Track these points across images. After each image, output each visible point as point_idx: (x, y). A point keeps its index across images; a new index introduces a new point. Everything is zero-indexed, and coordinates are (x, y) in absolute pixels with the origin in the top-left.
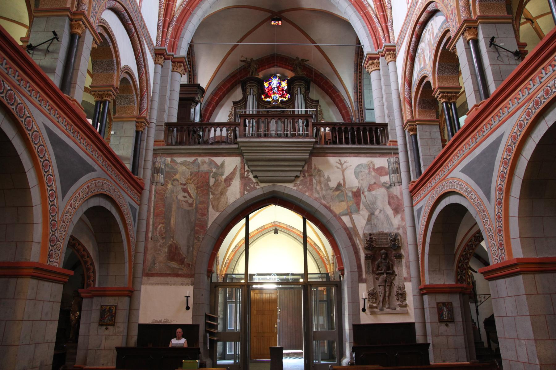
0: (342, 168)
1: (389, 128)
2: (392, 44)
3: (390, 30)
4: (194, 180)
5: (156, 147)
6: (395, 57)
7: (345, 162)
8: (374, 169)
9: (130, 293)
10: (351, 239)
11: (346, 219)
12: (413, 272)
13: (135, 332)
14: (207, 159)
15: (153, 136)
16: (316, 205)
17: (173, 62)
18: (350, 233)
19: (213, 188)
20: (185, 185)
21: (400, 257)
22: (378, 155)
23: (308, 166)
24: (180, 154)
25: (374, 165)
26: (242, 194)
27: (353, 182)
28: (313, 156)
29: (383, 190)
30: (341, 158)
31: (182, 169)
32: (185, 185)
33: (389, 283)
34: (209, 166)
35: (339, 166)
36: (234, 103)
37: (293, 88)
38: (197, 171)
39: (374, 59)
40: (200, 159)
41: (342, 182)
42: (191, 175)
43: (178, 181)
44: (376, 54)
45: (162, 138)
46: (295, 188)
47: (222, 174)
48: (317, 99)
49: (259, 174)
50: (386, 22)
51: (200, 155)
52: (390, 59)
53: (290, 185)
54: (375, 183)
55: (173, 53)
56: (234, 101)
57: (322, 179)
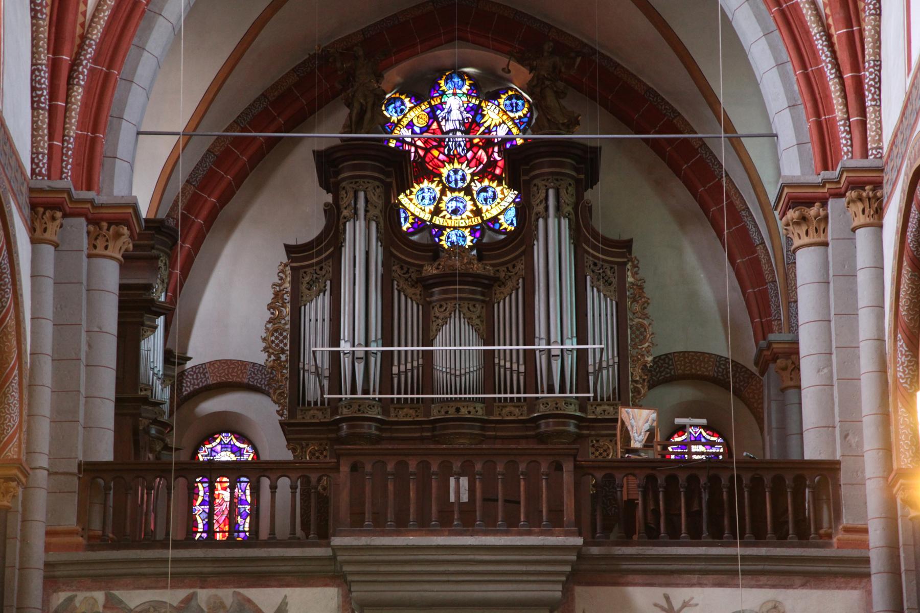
2: (871, 161)
17: (90, 221)
28: (580, 583)
39: (809, 202)
44: (817, 186)
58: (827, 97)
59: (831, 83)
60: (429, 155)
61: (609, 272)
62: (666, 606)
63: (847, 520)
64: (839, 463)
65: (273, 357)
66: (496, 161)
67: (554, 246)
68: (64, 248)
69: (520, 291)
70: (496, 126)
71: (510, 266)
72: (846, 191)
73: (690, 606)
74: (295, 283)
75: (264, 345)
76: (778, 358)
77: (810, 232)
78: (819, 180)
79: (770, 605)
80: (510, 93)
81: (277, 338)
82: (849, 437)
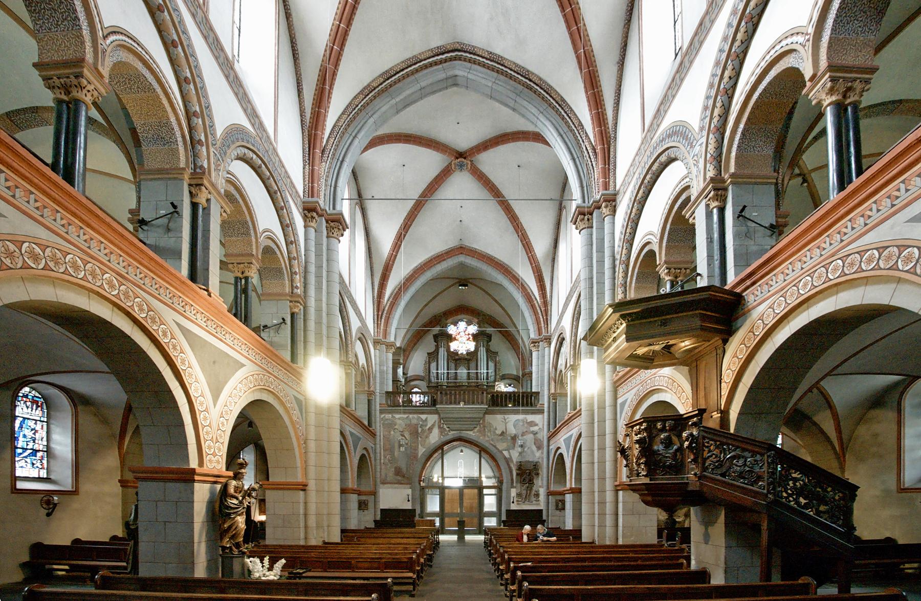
9: (374, 493)
10: (508, 465)
11: (506, 453)
12: (545, 483)
13: (379, 513)
14: (415, 416)
15: (378, 400)
16: (487, 445)
18: (508, 461)
21: (538, 474)
26: (440, 438)
27: (512, 430)
29: (532, 435)
31: (398, 422)
33: (530, 489)
40: (411, 416)
50: (547, 315)
51: (410, 413)
53: (471, 433)
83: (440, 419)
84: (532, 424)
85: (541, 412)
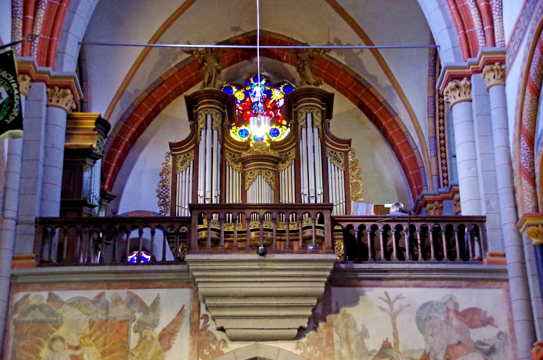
0: (392, 309)
1: (487, 225)
2: (498, 47)
3: (495, 17)
4: (97, 338)
5: (16, 271)
6: (504, 77)
7: (398, 298)
8: (456, 312)
14: (123, 293)
17: (48, 86)
19: (137, 354)
20: (77, 348)
22: (464, 283)
23: (324, 306)
24: (68, 285)
25: (456, 305)
30: (388, 290)
32: (77, 348)
34: (129, 306)
35: (386, 306)
36: (172, 145)
37: (296, 113)
38: (104, 318)
39: (461, 78)
40: (109, 294)
41: (391, 340)
42: (91, 328)
43: (62, 339)
44: (465, 68)
45: (28, 249)
46: (298, 352)
47: (154, 325)
48: (347, 138)
49: (226, 324)
51: (110, 284)
52: (493, 81)
54: (459, 343)
55: (49, 69)
56: (173, 141)
57: (352, 333)
58: (470, 20)
59: (472, 11)
60: (245, 113)
61: (339, 156)
62: (386, 298)
63: (491, 249)
64: (485, 217)
65: (162, 200)
66: (279, 116)
67: (310, 141)
68: (31, 99)
69: (293, 166)
70: (278, 100)
71: (288, 153)
72: (483, 68)
73: (401, 298)
74: (174, 162)
75: (157, 194)
76: (427, 203)
77: (462, 94)
78: (466, 64)
79: (448, 298)
80: (286, 84)
81: (164, 190)
82: (491, 203)
83: (198, 299)
84: (473, 317)
85: (494, 277)
